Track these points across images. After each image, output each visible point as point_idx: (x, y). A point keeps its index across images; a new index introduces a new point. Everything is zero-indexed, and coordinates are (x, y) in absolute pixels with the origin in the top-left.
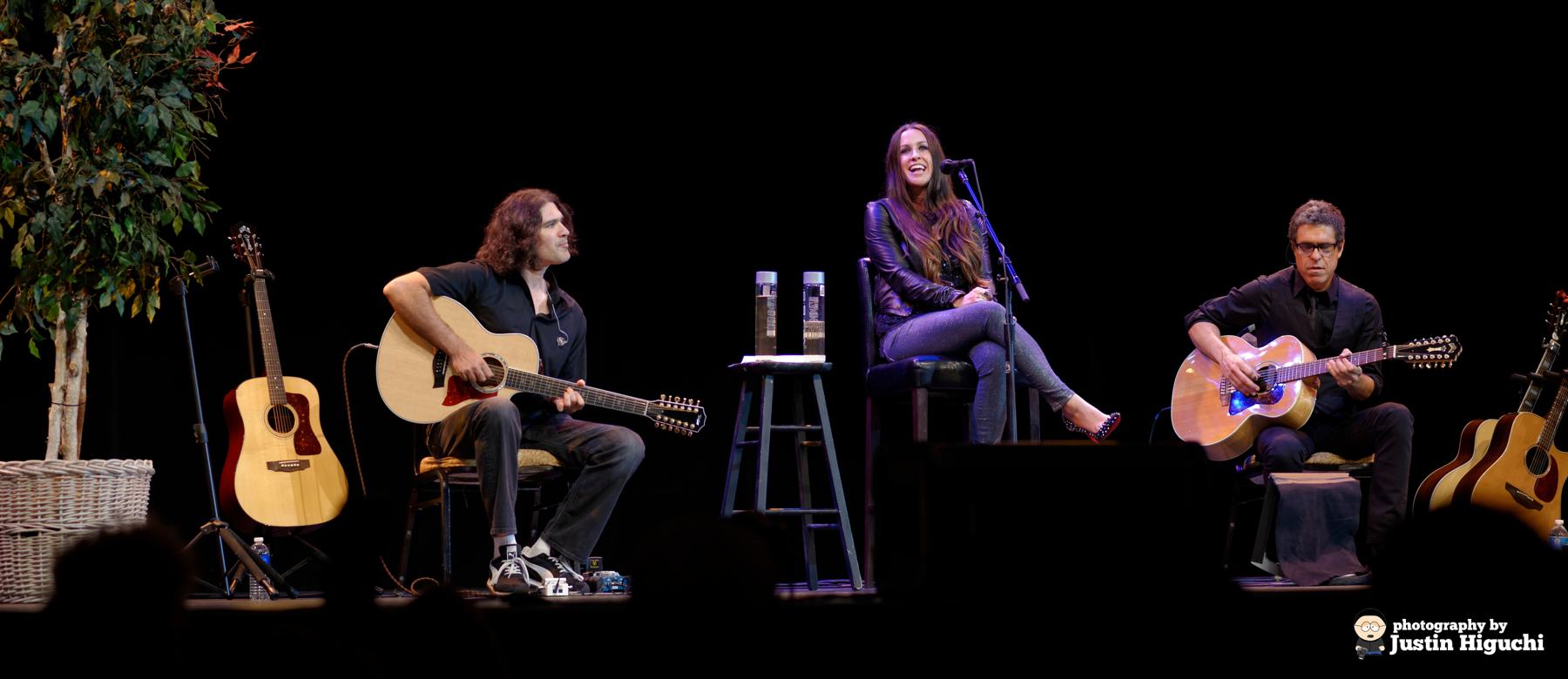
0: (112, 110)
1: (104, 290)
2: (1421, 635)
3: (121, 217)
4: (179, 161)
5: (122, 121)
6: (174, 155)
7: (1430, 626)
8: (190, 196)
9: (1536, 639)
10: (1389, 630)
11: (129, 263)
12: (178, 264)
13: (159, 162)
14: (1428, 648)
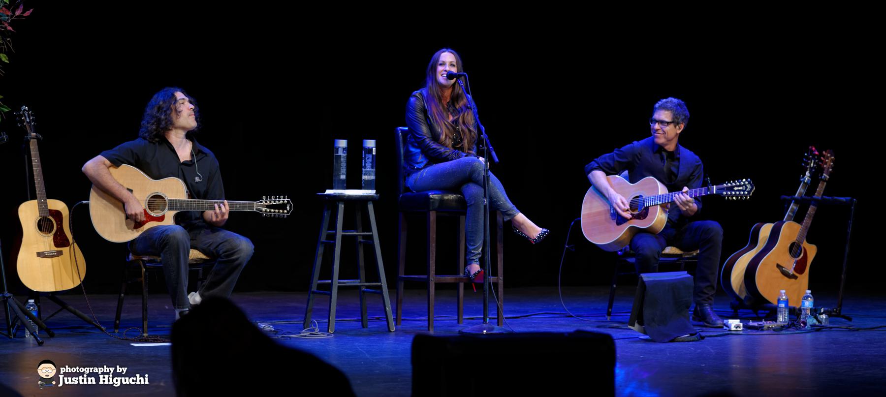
2: (77, 375)
7: (82, 370)
9: (144, 377)
10: (58, 372)
14: (81, 383)
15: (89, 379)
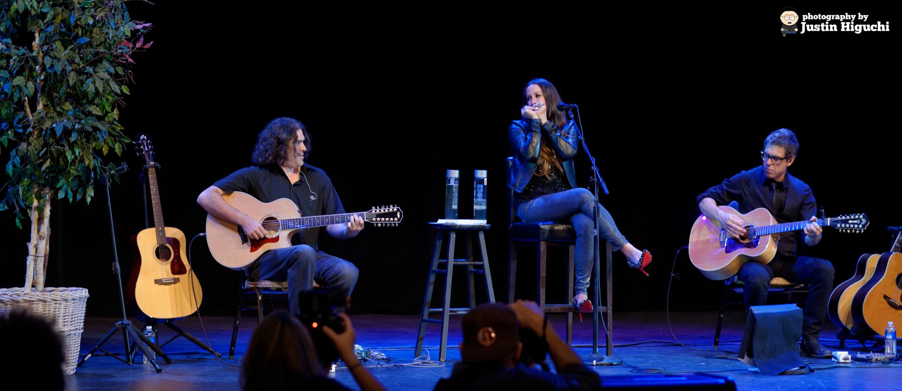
0: (67, 81)
1: (61, 188)
2: (819, 22)
3: (72, 146)
4: (107, 112)
5: (74, 87)
6: (104, 107)
7: (824, 17)
8: (113, 133)
11: (76, 173)
12: (105, 171)
13: (95, 112)
15: (831, 26)
